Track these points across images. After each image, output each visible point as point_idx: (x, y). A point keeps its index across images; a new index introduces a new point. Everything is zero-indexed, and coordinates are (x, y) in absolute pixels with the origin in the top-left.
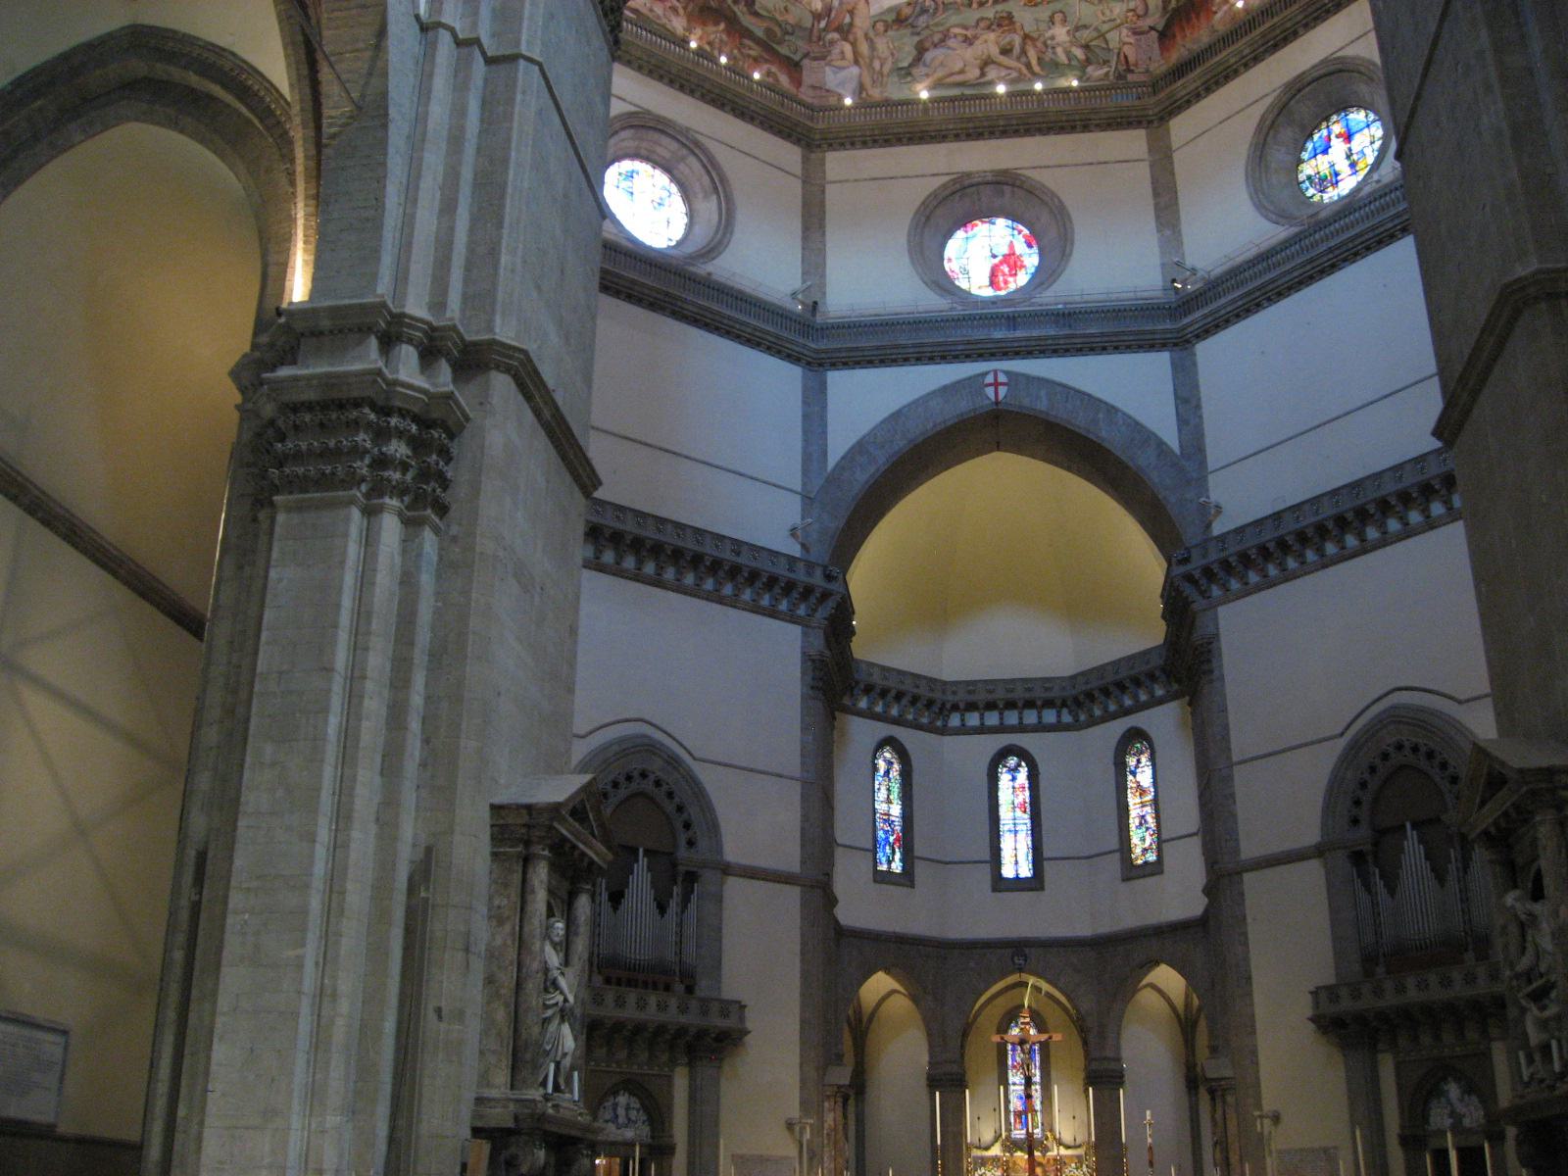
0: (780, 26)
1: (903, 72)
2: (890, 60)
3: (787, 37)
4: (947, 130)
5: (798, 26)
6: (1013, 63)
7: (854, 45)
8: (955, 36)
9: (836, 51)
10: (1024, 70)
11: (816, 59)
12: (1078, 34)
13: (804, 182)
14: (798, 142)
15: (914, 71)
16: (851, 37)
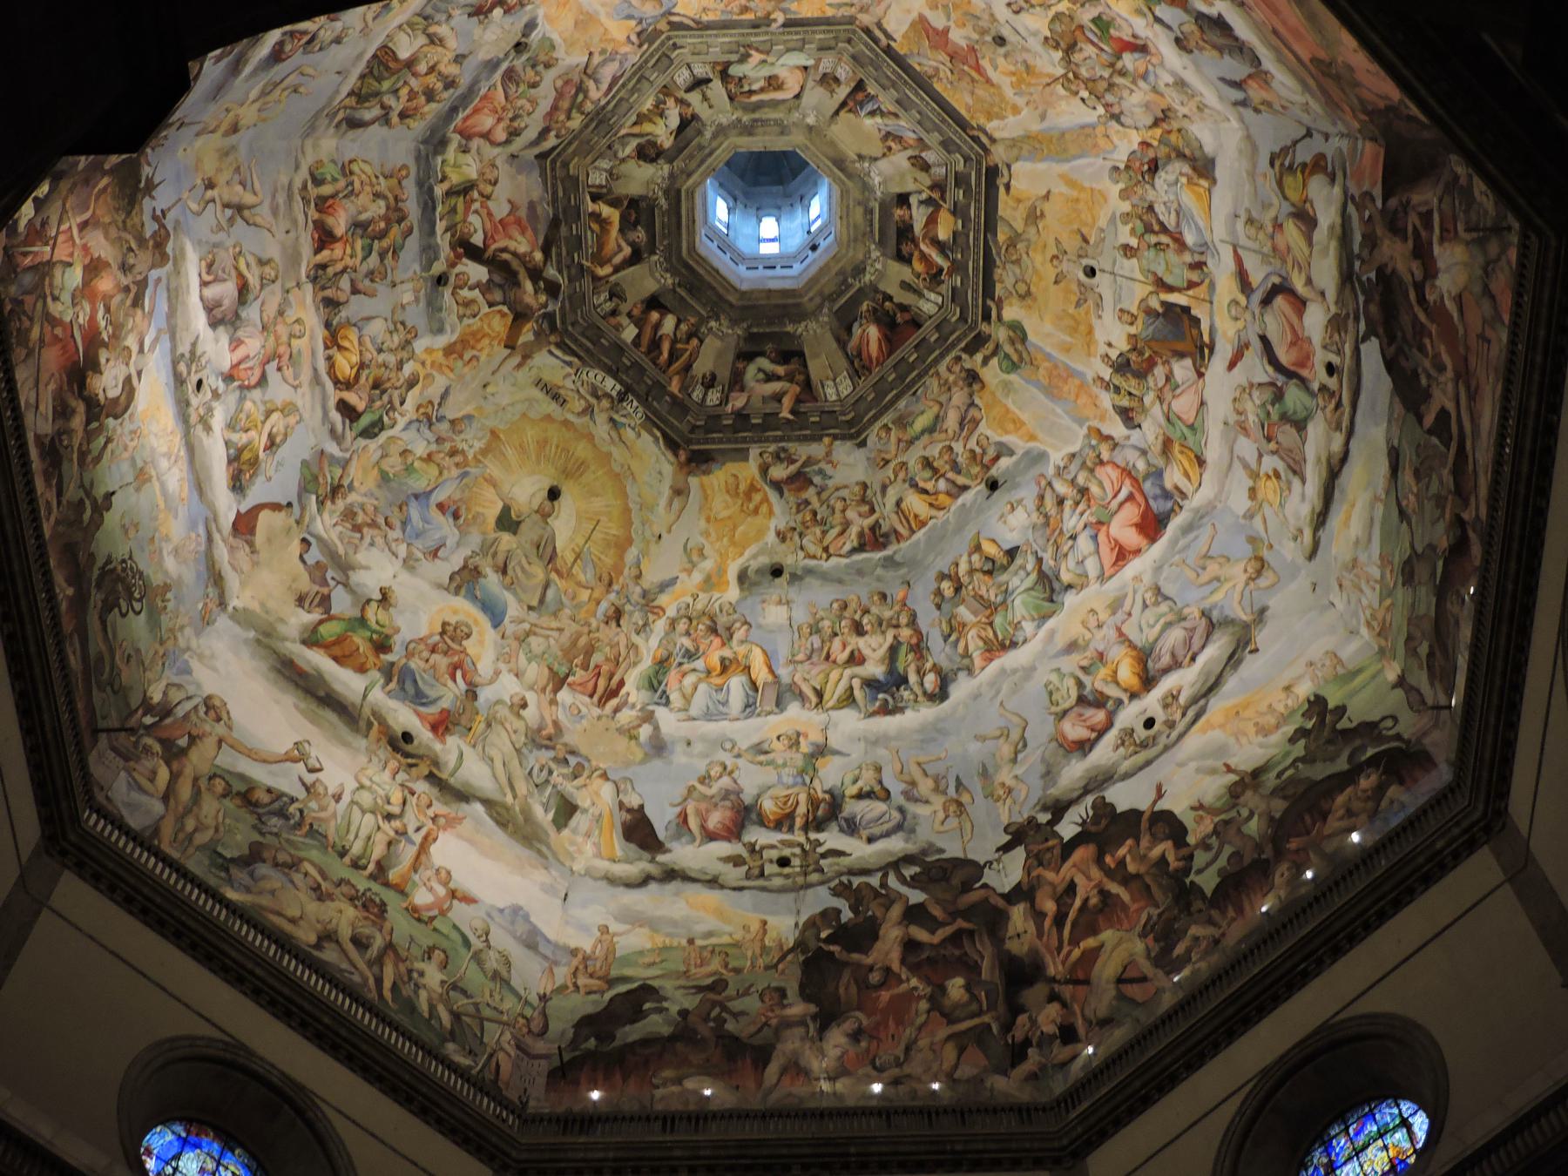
0: (112, 668)
1: (220, 861)
2: (211, 832)
3: (108, 689)
4: (252, 973)
5: (121, 692)
6: (362, 965)
7: (175, 777)
8: (306, 874)
9: (148, 763)
10: (371, 981)
11: (114, 749)
12: (452, 993)
13: (21, 876)
14: (46, 820)
15: (234, 871)
16: (175, 766)
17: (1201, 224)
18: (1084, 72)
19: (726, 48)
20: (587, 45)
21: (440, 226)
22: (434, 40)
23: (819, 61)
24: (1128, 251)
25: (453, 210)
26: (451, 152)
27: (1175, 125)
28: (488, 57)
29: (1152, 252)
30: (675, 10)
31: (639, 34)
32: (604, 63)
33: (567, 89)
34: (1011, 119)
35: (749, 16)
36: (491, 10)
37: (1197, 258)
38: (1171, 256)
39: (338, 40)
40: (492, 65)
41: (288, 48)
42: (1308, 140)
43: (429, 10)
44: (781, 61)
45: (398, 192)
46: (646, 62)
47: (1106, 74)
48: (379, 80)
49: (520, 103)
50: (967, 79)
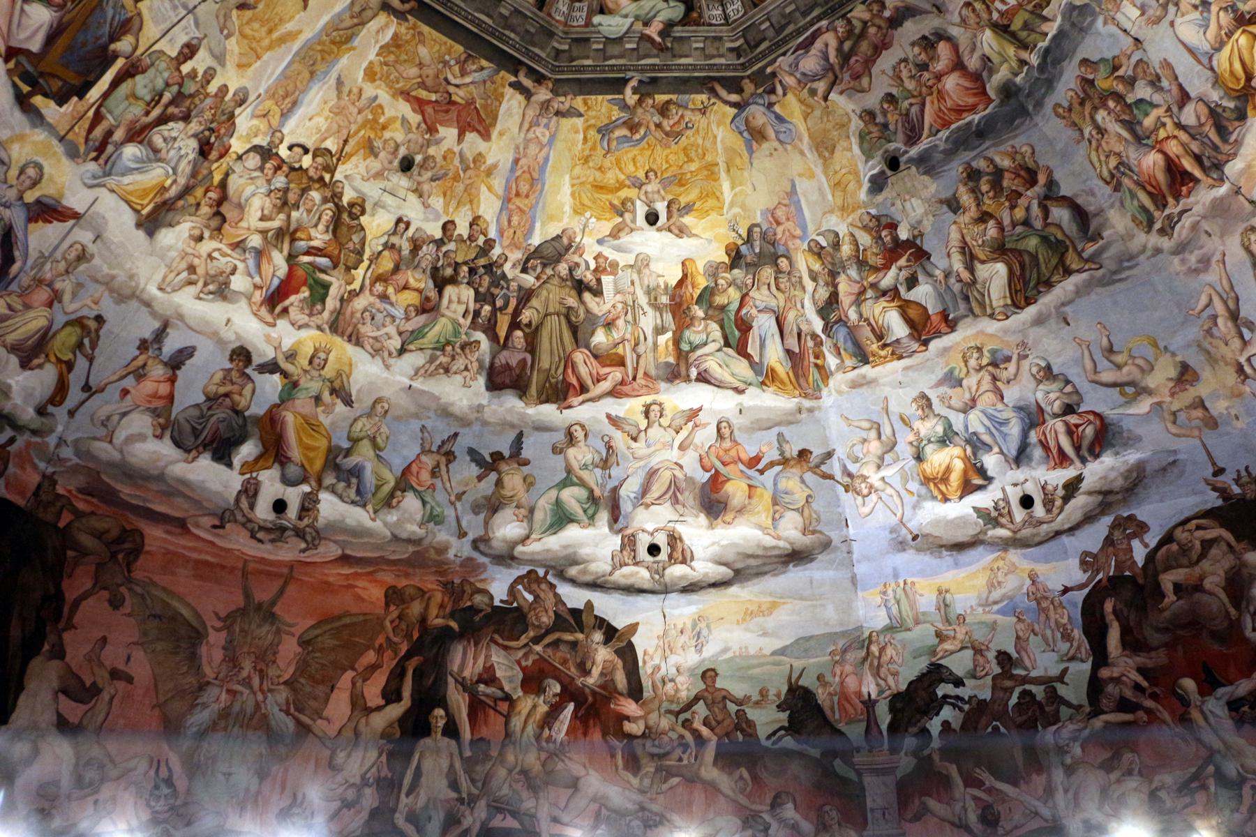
17: (126, 180)
18: (315, 195)
19: (685, 48)
20: (827, 112)
21: (1052, 29)
22: (970, 260)
23: (588, 23)
24: (189, 51)
25: (1026, 26)
26: (1002, 74)
27: (205, 210)
28: (926, 178)
29: (160, 83)
30: (733, 111)
31: (772, 91)
32: (815, 78)
33: (858, 67)
34: (372, 56)
35: (661, 98)
36: (909, 244)
37: (110, 149)
38: (137, 110)
39: (1048, 373)
40: (925, 163)
41: (1089, 431)
42: (83, 383)
43: (962, 306)
44: (630, 20)
45: (1076, 107)
46: (770, 50)
47: (295, 214)
48: (1034, 257)
49: (910, 85)
50: (429, 82)
